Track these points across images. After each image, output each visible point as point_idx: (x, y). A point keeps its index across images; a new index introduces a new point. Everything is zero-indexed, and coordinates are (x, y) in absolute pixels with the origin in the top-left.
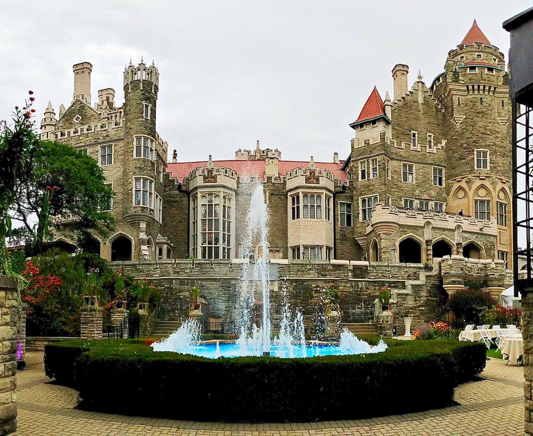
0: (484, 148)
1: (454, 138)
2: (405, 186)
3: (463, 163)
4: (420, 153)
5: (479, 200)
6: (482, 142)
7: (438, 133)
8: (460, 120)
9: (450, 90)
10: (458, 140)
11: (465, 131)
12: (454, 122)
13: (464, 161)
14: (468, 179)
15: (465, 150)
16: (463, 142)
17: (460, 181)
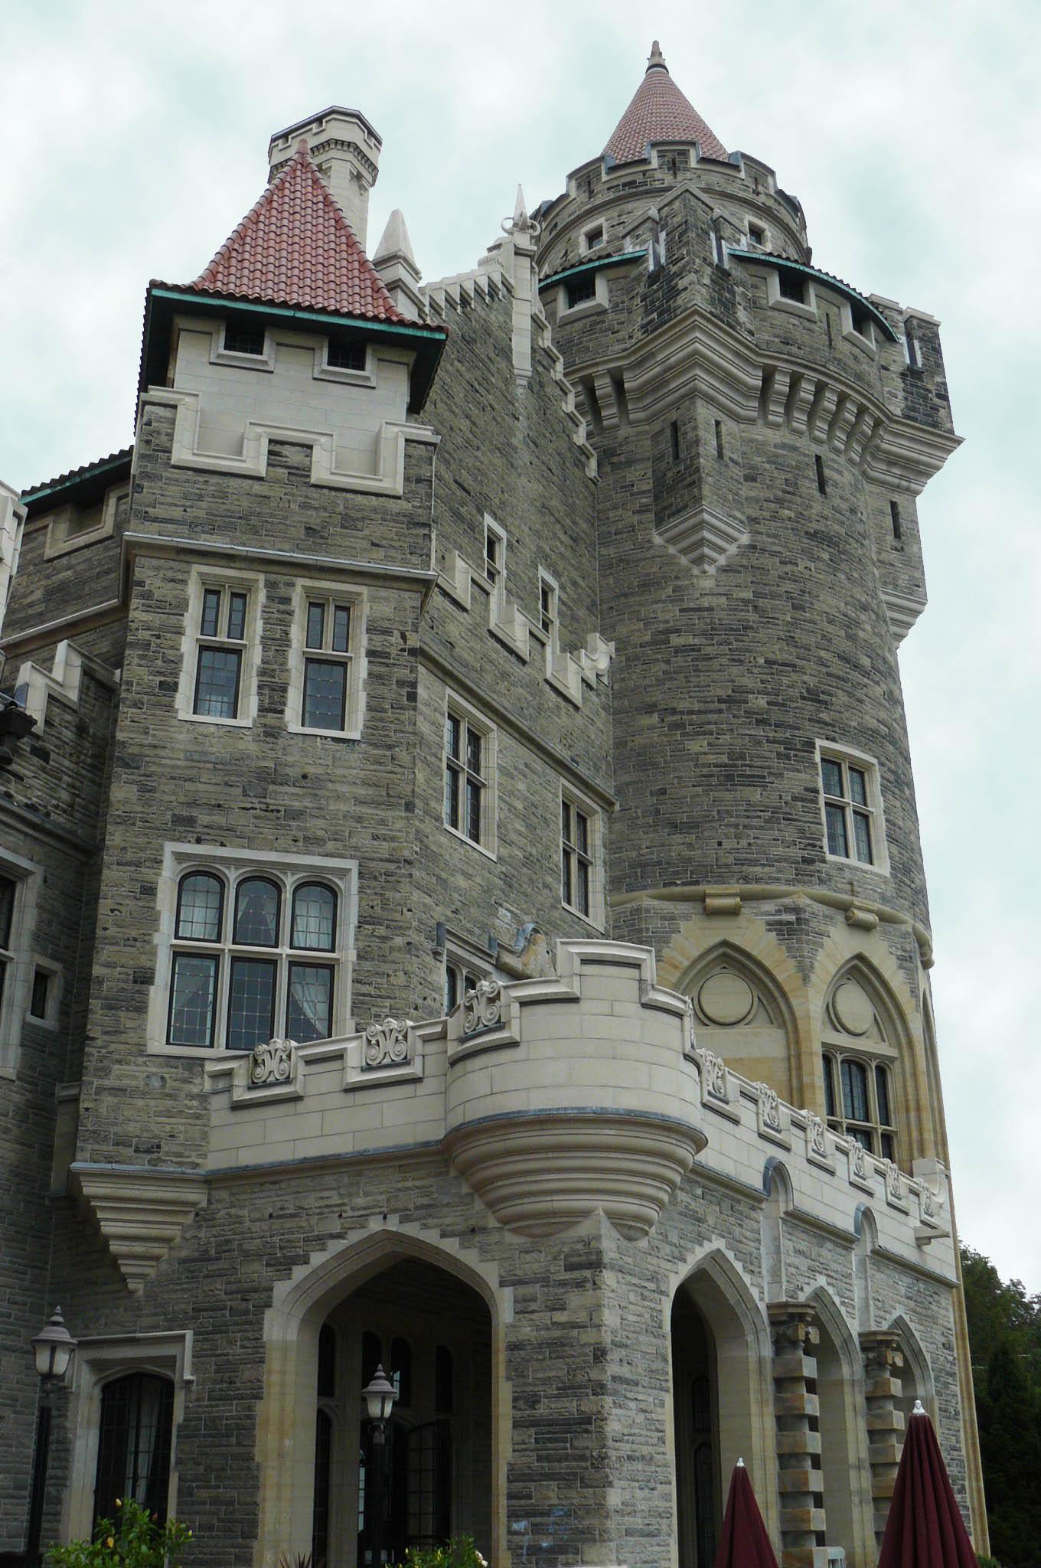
0: (858, 745)
1: (676, 640)
5: (842, 1049)
6: (849, 707)
7: (575, 584)
8: (721, 550)
9: (694, 360)
10: (708, 658)
11: (752, 617)
12: (672, 550)
13: (756, 795)
15: (759, 732)
16: (748, 682)
17: (733, 912)
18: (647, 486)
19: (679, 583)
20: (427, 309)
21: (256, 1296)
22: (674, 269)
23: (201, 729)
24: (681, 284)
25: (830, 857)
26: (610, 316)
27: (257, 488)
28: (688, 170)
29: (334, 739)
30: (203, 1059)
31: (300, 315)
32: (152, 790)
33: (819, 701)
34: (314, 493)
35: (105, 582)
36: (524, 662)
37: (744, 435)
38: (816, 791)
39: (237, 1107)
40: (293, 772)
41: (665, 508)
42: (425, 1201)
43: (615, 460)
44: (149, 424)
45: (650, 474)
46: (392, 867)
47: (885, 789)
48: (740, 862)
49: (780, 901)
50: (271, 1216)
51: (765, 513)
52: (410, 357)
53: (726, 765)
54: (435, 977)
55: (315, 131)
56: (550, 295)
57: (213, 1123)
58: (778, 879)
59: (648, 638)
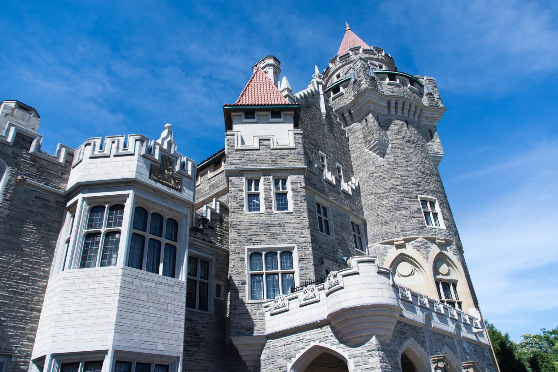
1: (375, 175)
2: (323, 241)
3: (403, 216)
4: (334, 188)
10: (384, 178)
11: (395, 166)
13: (403, 212)
14: (418, 242)
15: (402, 195)
16: (397, 183)
18: (362, 136)
19: (373, 160)
20: (296, 101)
21: (283, 368)
22: (359, 79)
23: (251, 215)
24: (362, 83)
25: (427, 226)
26: (345, 95)
27: (257, 152)
28: (359, 54)
29: (286, 213)
30: (261, 303)
31: (262, 107)
32: (240, 233)
33: (417, 185)
34: (272, 151)
35: (223, 182)
36: (335, 187)
37: (385, 119)
38: (421, 209)
39: (272, 315)
40: (277, 223)
41: (367, 141)
42: (325, 335)
43: (352, 131)
44: (228, 140)
45: (361, 133)
46: (306, 244)
47: (440, 205)
48: (402, 231)
49: (415, 240)
50: (284, 345)
51: (394, 138)
52: (293, 113)
53: (394, 206)
54: (322, 273)
55: (263, 63)
56: (328, 93)
57: (266, 320)
58: (414, 234)
59: (368, 176)
